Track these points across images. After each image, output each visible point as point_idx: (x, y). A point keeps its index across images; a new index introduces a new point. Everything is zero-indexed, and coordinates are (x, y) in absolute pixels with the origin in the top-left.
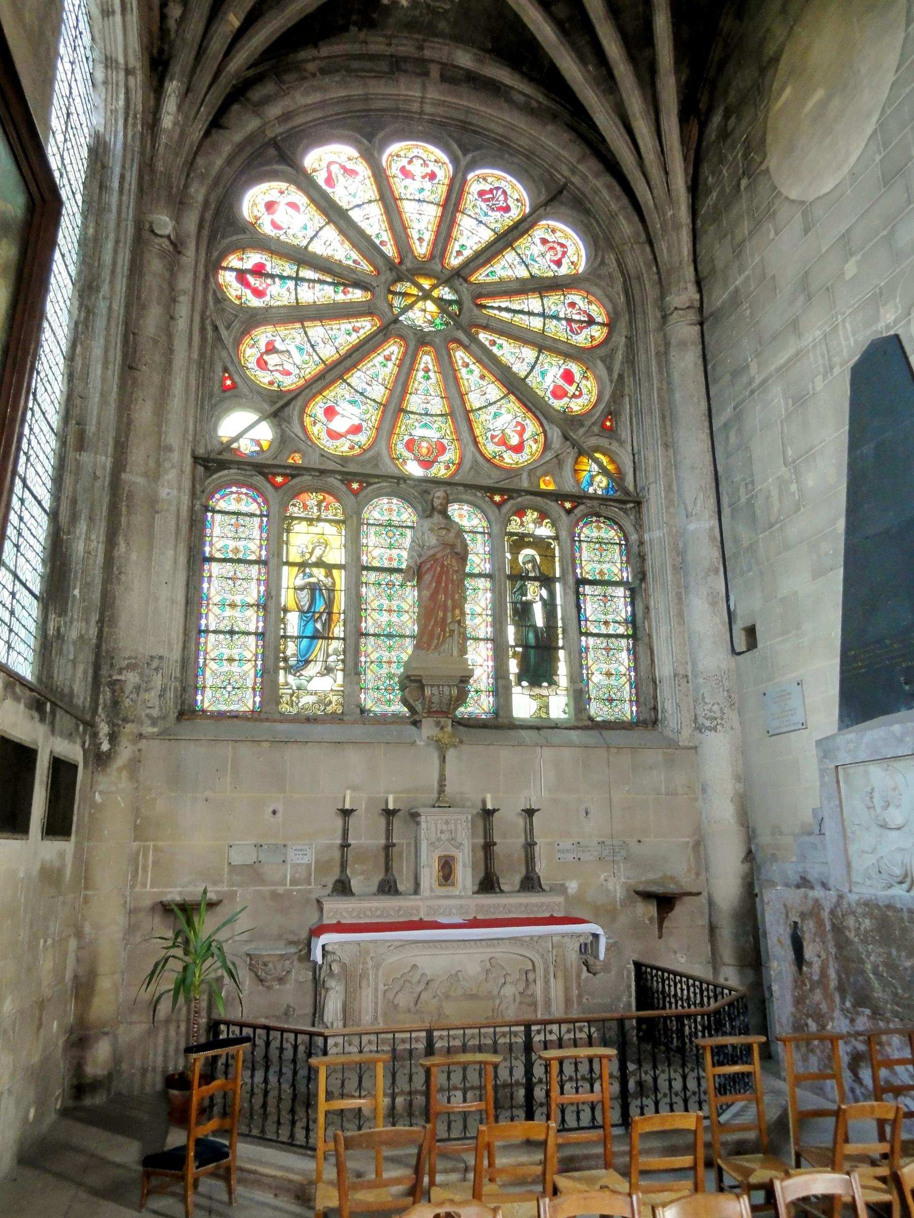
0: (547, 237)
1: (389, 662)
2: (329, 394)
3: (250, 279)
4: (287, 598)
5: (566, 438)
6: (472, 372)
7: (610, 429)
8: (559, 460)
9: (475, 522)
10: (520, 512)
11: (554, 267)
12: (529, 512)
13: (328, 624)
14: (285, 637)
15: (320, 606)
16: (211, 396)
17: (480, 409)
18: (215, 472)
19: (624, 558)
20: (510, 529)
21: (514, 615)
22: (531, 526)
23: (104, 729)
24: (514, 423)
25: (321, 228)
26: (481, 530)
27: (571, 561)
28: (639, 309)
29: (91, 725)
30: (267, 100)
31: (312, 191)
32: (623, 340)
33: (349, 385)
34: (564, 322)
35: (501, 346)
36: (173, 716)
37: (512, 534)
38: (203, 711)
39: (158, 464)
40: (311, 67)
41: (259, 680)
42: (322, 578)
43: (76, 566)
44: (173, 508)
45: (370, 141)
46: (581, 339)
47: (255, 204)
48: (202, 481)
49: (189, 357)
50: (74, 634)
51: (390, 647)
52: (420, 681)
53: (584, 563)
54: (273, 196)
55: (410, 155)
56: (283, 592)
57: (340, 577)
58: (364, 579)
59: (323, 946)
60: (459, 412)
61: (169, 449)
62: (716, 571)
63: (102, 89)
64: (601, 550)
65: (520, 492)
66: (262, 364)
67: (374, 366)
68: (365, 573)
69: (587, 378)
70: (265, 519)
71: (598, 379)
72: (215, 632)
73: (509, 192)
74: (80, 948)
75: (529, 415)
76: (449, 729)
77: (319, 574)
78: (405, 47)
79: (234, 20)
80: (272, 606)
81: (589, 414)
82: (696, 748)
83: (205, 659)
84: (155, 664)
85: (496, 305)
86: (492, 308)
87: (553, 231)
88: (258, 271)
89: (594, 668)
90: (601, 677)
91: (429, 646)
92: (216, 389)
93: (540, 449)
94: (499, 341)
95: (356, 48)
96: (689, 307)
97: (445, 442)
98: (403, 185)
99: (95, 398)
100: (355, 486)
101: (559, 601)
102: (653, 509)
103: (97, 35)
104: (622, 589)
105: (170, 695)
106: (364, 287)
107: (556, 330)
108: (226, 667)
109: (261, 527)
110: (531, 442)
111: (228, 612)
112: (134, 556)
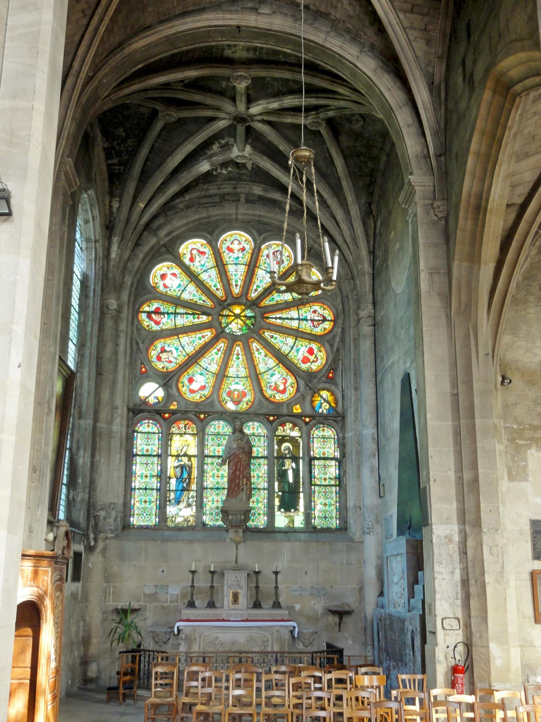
2: (190, 371)
3: (153, 316)
4: (171, 472)
6: (261, 353)
7: (332, 378)
8: (303, 398)
9: (260, 431)
10: (283, 424)
12: (287, 424)
13: (189, 484)
14: (169, 491)
15: (185, 475)
16: (135, 377)
19: (336, 446)
20: (277, 433)
22: (289, 431)
23: (92, 536)
26: (263, 434)
27: (308, 448)
28: (347, 314)
29: (87, 536)
30: (160, 227)
31: (183, 267)
32: (340, 329)
34: (310, 322)
35: (276, 338)
36: (120, 528)
37: (278, 436)
38: (134, 526)
39: (112, 416)
40: (181, 206)
41: (158, 511)
43: (80, 470)
44: (119, 435)
45: (211, 236)
46: (318, 331)
47: (155, 276)
48: (132, 419)
49: (125, 362)
50: (79, 498)
52: (227, 512)
54: (164, 270)
55: (232, 239)
57: (194, 461)
58: (206, 462)
59: (178, 627)
60: (253, 376)
61: (117, 408)
62: (374, 455)
63: (85, 252)
64: (324, 442)
65: (283, 416)
66: (159, 358)
69: (321, 351)
72: (139, 489)
74: (84, 626)
75: (289, 373)
76: (241, 534)
77: (185, 460)
78: (227, 189)
79: (142, 205)
80: (163, 477)
81: (319, 371)
82: (362, 542)
84: (112, 507)
85: (274, 316)
86: (272, 318)
88: (157, 312)
89: (318, 502)
91: (232, 494)
92: (138, 373)
93: (294, 391)
94: (275, 336)
95: (203, 193)
96: (369, 317)
97: (246, 391)
99: (86, 395)
100: (202, 416)
103: (83, 231)
105: (119, 519)
106: (208, 314)
107: (306, 327)
109: (158, 439)
110: (290, 388)
111: (144, 480)
112: (102, 460)
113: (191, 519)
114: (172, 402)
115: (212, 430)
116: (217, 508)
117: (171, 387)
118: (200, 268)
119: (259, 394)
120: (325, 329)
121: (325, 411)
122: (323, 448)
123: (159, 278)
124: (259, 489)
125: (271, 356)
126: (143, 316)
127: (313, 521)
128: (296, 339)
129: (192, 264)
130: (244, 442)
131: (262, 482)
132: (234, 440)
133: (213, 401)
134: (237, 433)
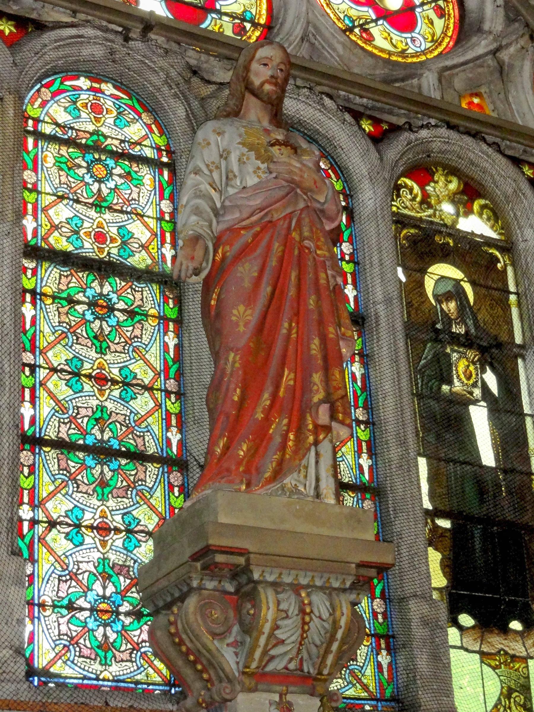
22: (448, 208)
51: (103, 483)
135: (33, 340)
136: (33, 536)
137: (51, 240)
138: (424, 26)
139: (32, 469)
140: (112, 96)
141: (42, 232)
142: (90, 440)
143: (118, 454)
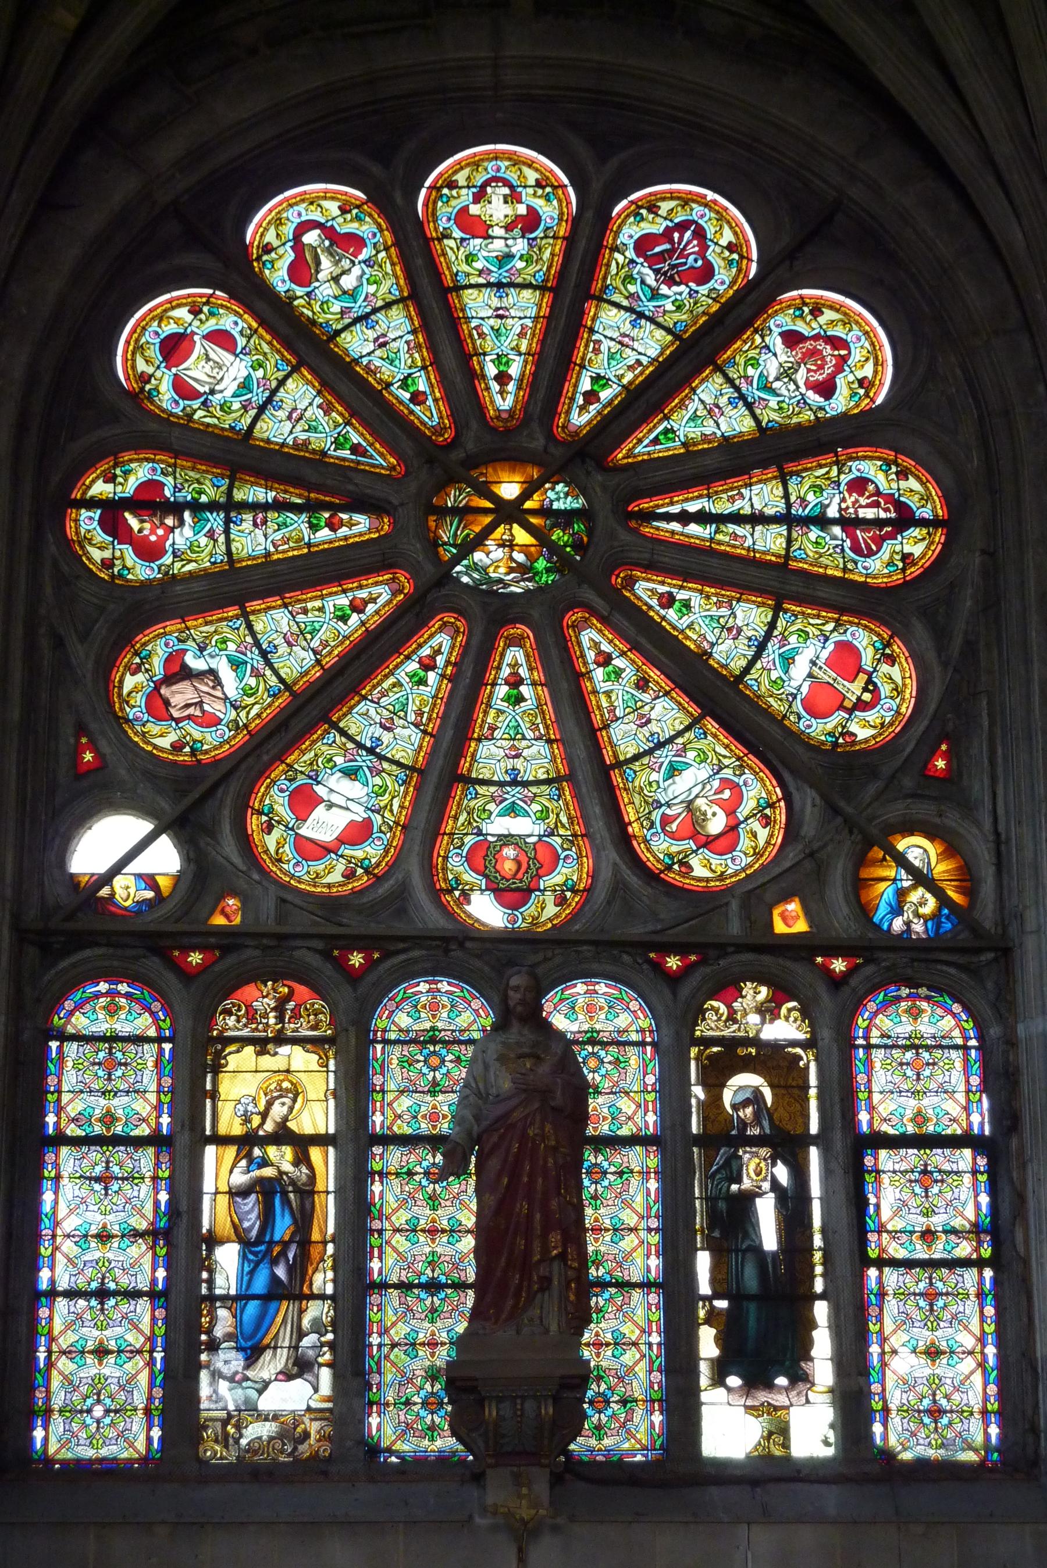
0: (801, 327)
1: (433, 1344)
2: (300, 760)
5: (834, 810)
6: (618, 673)
11: (813, 397)
12: (748, 988)
13: (300, 1269)
14: (212, 1298)
15: (283, 1226)
17: (636, 757)
18: (65, 953)
19: (975, 1081)
21: (711, 1227)
22: (754, 1019)
24: (716, 784)
25: (282, 383)
26: (635, 1037)
31: (260, 305)
33: (343, 733)
34: (837, 530)
35: (687, 605)
41: (158, 1393)
42: (287, 1167)
47: (139, 348)
51: (433, 1310)
52: (473, 1390)
53: (876, 1098)
55: (480, 179)
56: (206, 1201)
60: (585, 773)
65: (722, 949)
67: (398, 684)
68: (377, 1150)
69: (891, 660)
70: (167, 1047)
71: (916, 657)
72: (71, 1294)
73: (710, 230)
75: (752, 760)
76: (542, 1488)
77: (282, 1157)
83: (49, 1352)
85: (675, 509)
86: (668, 517)
87: (816, 312)
89: (896, 1341)
90: (913, 1359)
97: (555, 842)
98: (461, 255)
100: (356, 959)
101: (815, 1188)
102: (1031, 966)
104: (967, 1153)
108: (91, 1368)
109: (158, 1063)
110: (755, 825)
111: (95, 1252)
113: (314, 1427)
114: (222, 897)
115: (403, 1020)
116: (432, 1376)
117: (212, 832)
118: (336, 307)
119: (612, 855)
120: (906, 557)
121: (918, 927)
122: (915, 1093)
123: (154, 352)
124: (625, 1286)
125: (666, 684)
126: (88, 521)
127: (877, 1428)
128: (777, 610)
129: (300, 291)
130: (544, 1069)
131: (639, 1257)
132: (502, 1059)
133: (402, 893)
134: (515, 1027)
135: (380, 1211)
136: (380, 1357)
137: (395, 1128)
138: (747, 841)
139: (379, 1306)
140: (446, 992)
141: (387, 1123)
142: (423, 1279)
143: (447, 1286)
